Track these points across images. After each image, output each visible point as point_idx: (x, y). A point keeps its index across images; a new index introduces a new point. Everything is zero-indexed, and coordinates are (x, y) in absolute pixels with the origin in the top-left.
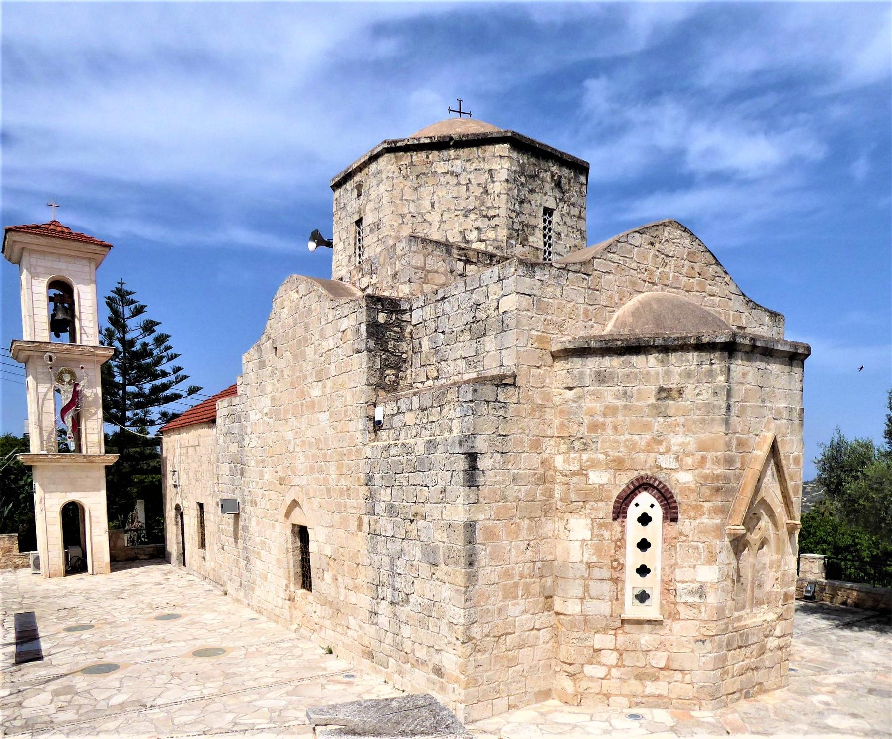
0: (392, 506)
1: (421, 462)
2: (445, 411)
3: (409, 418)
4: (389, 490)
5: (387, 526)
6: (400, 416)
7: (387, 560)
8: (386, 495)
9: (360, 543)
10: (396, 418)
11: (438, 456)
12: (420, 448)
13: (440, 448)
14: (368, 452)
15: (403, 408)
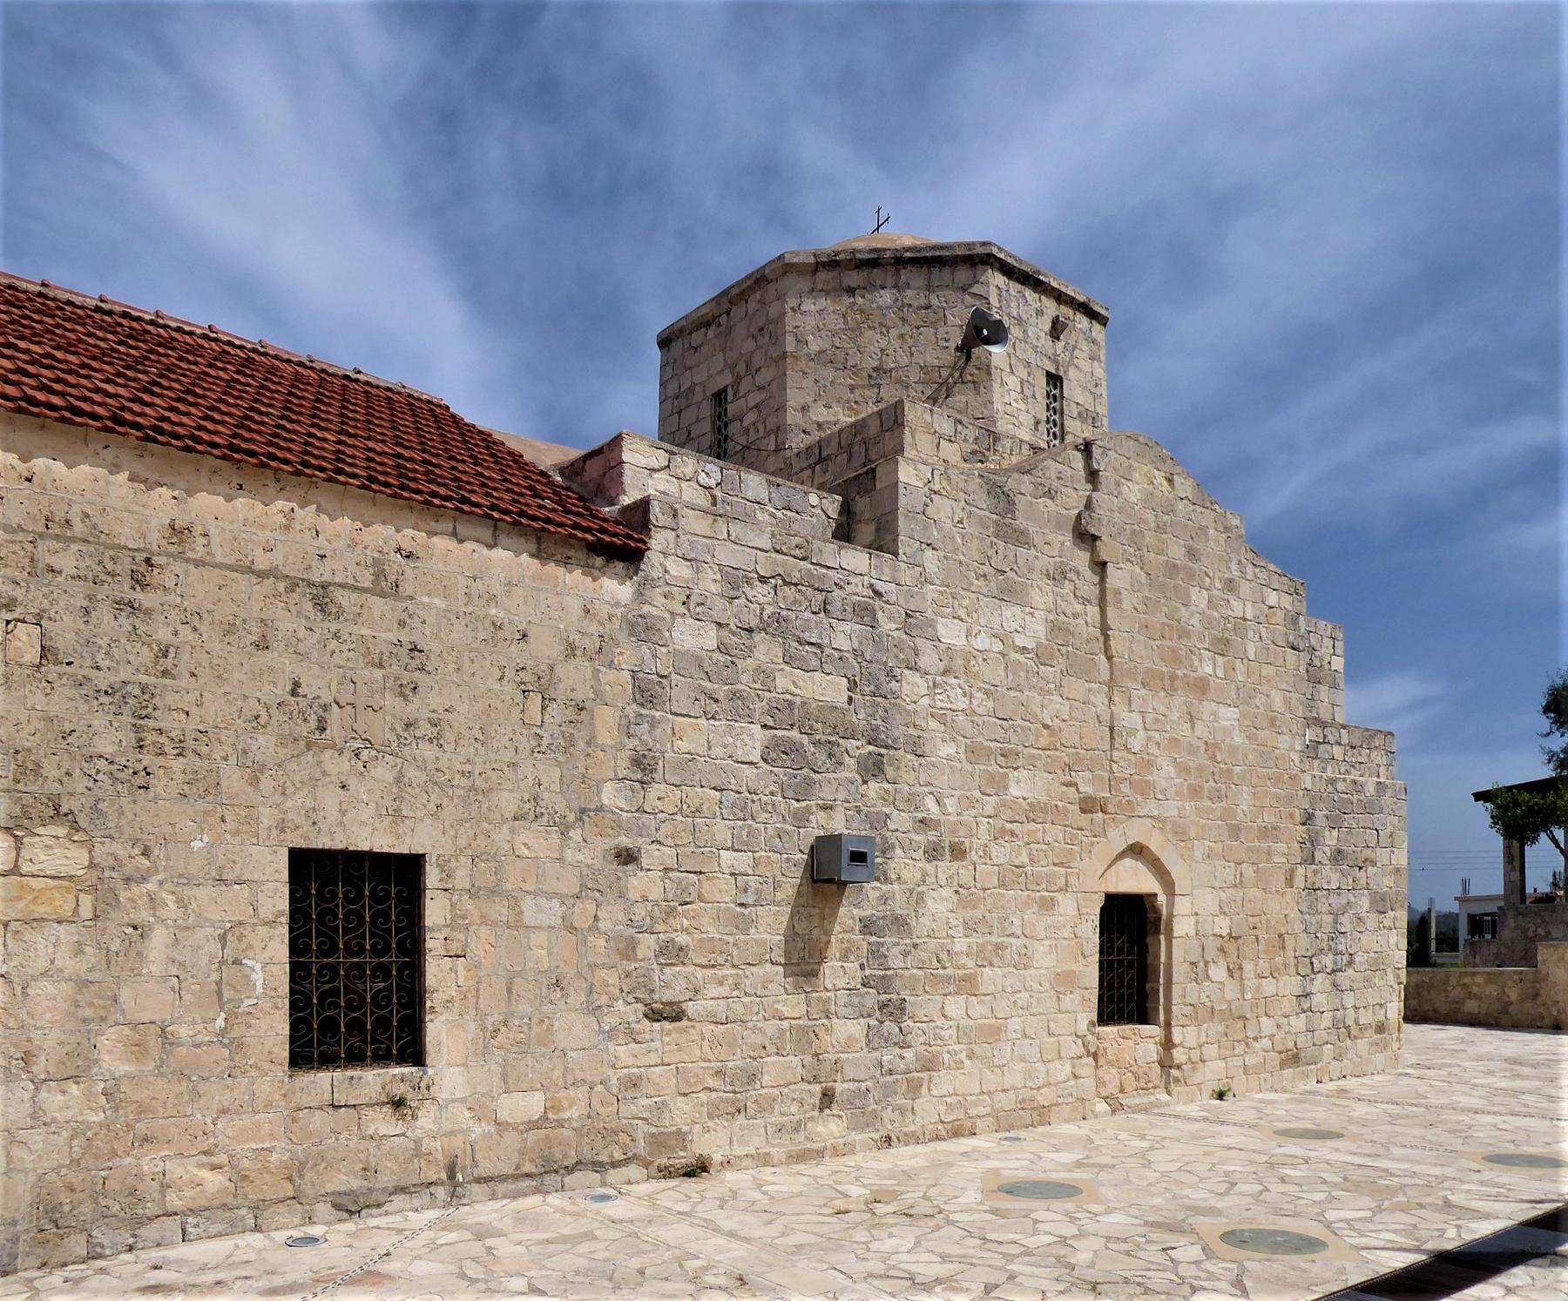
0: (1340, 852)
1: (1371, 802)
2: (1374, 754)
3: (1337, 751)
4: (1335, 833)
5: (1332, 877)
6: (1328, 747)
7: (1328, 919)
8: (1331, 838)
9: (1283, 907)
10: (1321, 747)
11: (1387, 799)
12: (1370, 789)
13: (1389, 793)
14: (1307, 781)
15: (1331, 738)
